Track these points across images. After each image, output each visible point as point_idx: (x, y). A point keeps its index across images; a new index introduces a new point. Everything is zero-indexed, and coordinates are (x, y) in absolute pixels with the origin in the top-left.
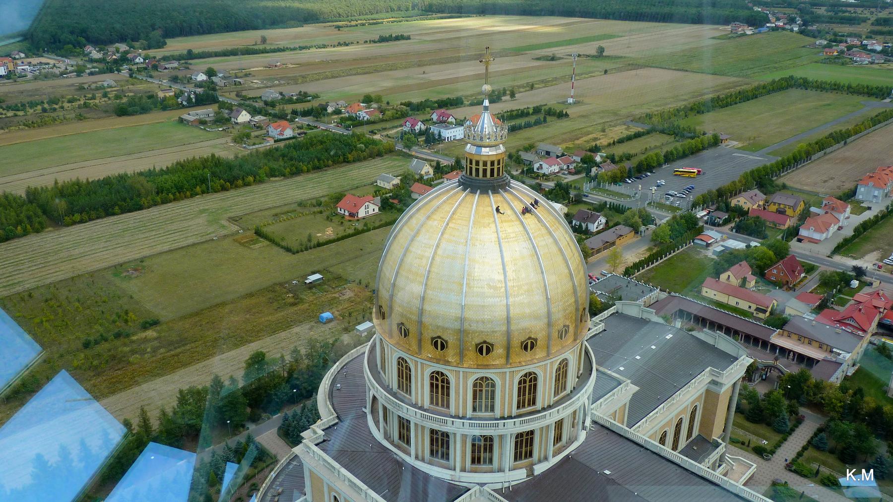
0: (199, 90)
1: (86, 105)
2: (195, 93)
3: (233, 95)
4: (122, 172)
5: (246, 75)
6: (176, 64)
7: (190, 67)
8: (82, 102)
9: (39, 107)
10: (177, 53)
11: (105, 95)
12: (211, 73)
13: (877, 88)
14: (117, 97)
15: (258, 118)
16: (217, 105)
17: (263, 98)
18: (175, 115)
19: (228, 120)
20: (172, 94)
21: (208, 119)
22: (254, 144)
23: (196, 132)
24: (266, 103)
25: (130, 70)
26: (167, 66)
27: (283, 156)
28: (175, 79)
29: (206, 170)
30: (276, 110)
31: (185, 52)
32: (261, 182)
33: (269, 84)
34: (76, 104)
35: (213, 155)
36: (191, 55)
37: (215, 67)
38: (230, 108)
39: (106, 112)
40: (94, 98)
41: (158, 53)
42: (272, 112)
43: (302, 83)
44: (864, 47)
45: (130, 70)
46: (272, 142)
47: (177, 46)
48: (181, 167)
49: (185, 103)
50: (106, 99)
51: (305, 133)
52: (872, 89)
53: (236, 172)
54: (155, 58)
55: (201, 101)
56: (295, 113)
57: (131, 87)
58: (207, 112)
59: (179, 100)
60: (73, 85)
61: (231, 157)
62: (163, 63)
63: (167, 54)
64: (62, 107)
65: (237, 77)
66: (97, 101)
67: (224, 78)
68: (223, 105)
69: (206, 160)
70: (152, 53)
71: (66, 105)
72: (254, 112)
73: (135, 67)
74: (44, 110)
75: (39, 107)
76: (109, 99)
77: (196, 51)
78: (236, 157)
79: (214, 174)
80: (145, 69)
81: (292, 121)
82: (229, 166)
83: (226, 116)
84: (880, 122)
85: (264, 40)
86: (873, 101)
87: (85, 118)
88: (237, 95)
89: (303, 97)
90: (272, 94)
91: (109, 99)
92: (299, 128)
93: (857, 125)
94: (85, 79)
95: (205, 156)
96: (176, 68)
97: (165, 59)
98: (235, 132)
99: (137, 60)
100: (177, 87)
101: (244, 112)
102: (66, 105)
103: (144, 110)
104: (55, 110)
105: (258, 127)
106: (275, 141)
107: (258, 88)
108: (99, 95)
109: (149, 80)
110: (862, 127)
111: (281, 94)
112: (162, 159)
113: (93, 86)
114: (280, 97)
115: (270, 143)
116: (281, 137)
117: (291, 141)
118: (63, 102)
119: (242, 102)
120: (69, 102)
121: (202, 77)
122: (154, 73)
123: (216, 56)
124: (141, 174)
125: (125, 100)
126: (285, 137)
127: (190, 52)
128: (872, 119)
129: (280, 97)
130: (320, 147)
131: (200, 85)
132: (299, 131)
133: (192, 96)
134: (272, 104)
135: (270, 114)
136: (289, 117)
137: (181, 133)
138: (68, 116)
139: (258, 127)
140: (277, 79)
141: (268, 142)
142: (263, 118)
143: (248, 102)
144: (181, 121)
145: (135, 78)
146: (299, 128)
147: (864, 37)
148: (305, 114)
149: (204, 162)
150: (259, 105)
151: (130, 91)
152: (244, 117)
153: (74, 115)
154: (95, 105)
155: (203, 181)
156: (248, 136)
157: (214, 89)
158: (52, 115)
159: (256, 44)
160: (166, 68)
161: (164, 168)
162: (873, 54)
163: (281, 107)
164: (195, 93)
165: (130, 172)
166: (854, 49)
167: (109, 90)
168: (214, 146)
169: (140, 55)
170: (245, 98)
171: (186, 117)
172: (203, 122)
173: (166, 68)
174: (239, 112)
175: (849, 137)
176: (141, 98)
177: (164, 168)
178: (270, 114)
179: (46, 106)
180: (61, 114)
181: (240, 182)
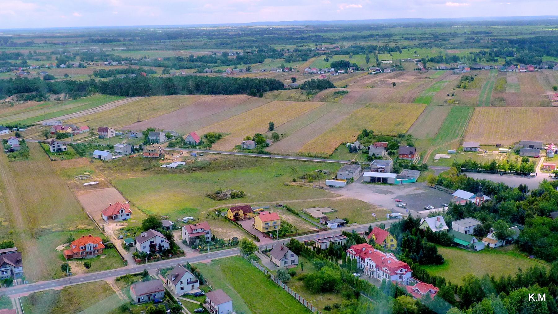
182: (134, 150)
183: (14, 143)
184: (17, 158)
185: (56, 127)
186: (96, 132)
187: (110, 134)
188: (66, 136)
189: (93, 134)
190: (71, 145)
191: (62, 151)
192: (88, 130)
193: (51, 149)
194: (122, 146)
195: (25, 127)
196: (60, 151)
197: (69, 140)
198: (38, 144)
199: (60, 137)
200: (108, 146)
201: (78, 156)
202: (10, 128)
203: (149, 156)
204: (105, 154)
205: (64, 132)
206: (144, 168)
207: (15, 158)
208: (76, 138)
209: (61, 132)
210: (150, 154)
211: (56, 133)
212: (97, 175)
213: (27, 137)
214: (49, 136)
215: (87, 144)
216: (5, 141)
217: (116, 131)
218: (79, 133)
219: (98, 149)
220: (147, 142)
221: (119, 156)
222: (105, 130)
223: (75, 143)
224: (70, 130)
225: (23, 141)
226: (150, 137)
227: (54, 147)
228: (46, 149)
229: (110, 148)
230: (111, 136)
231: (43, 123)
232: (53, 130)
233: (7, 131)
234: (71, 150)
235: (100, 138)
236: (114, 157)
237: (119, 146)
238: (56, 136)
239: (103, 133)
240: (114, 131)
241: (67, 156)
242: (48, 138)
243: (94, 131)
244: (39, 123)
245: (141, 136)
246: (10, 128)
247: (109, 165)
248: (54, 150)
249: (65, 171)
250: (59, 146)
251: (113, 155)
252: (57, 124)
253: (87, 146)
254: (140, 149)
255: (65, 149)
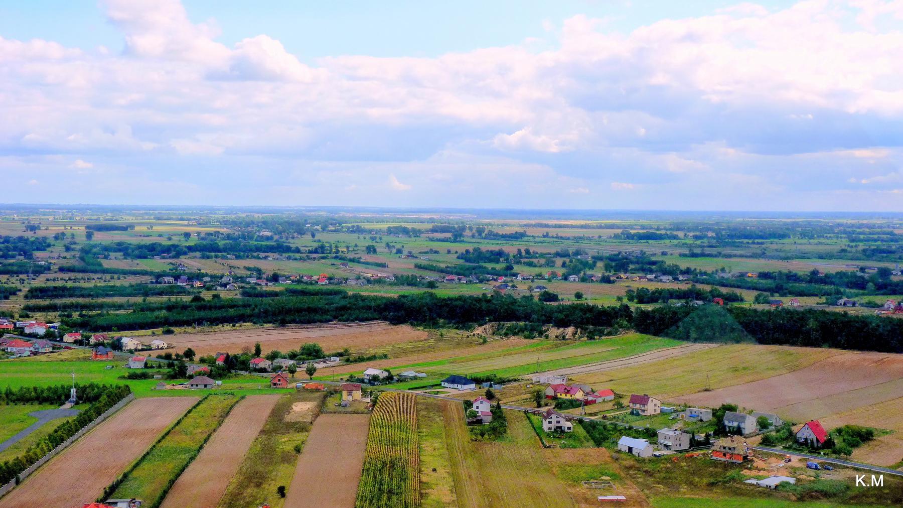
13: (49, 389)
44: (21, 331)
52: (42, 391)
84: (62, 440)
86: (48, 408)
93: (29, 450)
110: (38, 451)
128: (50, 436)
147: (17, 316)
162: (34, 340)
166: (6, 336)
175: (21, 470)
182: (695, 444)
183: (483, 408)
184: (486, 436)
185: (556, 388)
186: (625, 402)
187: (651, 408)
188: (574, 404)
189: (620, 406)
190: (581, 422)
191: (563, 432)
192: (612, 397)
193: (545, 425)
194: (672, 433)
195: (502, 382)
196: (559, 432)
197: (576, 412)
198: (523, 415)
199: (561, 405)
200: (647, 430)
201: (592, 443)
202: (477, 381)
203: (723, 459)
204: (641, 446)
205: (569, 397)
206: (712, 480)
207: (482, 435)
208: (590, 409)
209: (563, 396)
210: (725, 455)
211: (555, 398)
212: (623, 484)
213: (505, 401)
214: (542, 403)
215: (608, 422)
216: (468, 404)
217: (663, 404)
218: (594, 402)
219: (629, 435)
220: (721, 431)
221: (665, 452)
222: (643, 400)
223: (587, 419)
224: (579, 395)
225: (499, 406)
226: (727, 423)
227: (550, 422)
228: (536, 424)
229: (651, 435)
230: (653, 413)
231: (534, 378)
232: (550, 392)
233: (473, 386)
234: (581, 431)
235: (632, 413)
236: (657, 453)
237: (667, 434)
238: (554, 403)
239: (638, 406)
240: (659, 403)
241: (572, 442)
242: (539, 406)
243: (622, 401)
244: (527, 377)
245: (708, 417)
246: (477, 381)
247: (648, 467)
248: (550, 428)
249: (568, 469)
250: (558, 422)
251: (655, 450)
252: (558, 382)
253: (609, 427)
254: (706, 443)
255: (569, 428)
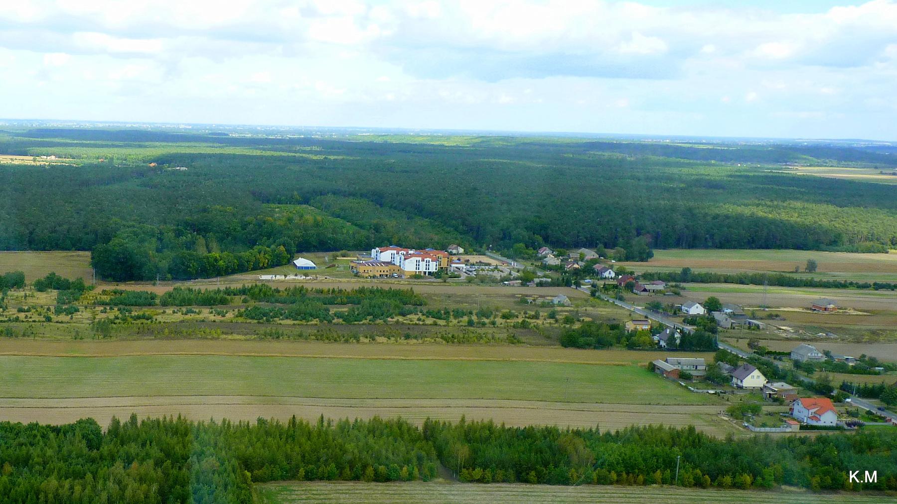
0: (689, 328)
1: (524, 325)
2: (682, 332)
3: (744, 343)
4: (551, 424)
5: (771, 317)
6: (660, 286)
7: (682, 293)
8: (520, 320)
9: (466, 319)
10: (667, 271)
11: (552, 316)
12: (712, 306)
14: (568, 320)
15: (777, 386)
16: (713, 354)
17: (794, 356)
18: (644, 358)
19: (727, 380)
20: (647, 327)
21: (694, 373)
22: (764, 425)
23: (672, 389)
24: (797, 364)
25: (594, 286)
26: (647, 287)
27: (813, 455)
28: (655, 308)
29: (676, 449)
30: (815, 378)
31: (679, 271)
32: (764, 487)
33: (809, 335)
34: (512, 321)
35: (691, 429)
36: (686, 276)
37: (722, 298)
38: (734, 361)
39: (548, 337)
40: (536, 317)
41: (637, 268)
42: (806, 380)
43: (870, 342)
45: (594, 286)
46: (795, 427)
47: (667, 260)
48: (639, 436)
49: (663, 343)
50: (552, 321)
51: (860, 425)
53: (725, 462)
54: (632, 273)
55: (688, 344)
56: (846, 389)
57: (589, 309)
58: (695, 362)
59: (656, 338)
60: (513, 296)
61: (721, 437)
62: (641, 282)
63: (651, 270)
64: (493, 323)
65: (754, 318)
66: (540, 322)
67: (733, 315)
68: (723, 356)
69: (679, 434)
70: (629, 266)
71: (499, 320)
72: (772, 375)
73: (601, 283)
74: (471, 323)
75: (466, 319)
76: (557, 321)
77: (695, 271)
78: (730, 440)
79: (687, 458)
80: (615, 287)
81: (838, 400)
82: (716, 451)
83: (725, 373)
85: (812, 267)
87: (519, 342)
88: (750, 345)
89: (867, 366)
90: (812, 352)
91: (557, 321)
92: (849, 414)
94: (532, 290)
95: (679, 428)
96: (660, 292)
97: (648, 277)
98: (735, 400)
99: (606, 274)
100: (655, 319)
101: (756, 373)
102: (499, 320)
103: (601, 344)
104: (484, 324)
105: (775, 400)
106: (802, 428)
107: (787, 339)
108: (543, 313)
109: (618, 303)
111: (827, 354)
112: (613, 419)
113: (540, 301)
114: (824, 359)
115: (793, 429)
116: (815, 423)
117: (831, 433)
118: (496, 316)
119: (757, 356)
120: (504, 317)
121: (697, 310)
122: (626, 295)
123: (726, 282)
124: (577, 433)
125: (577, 326)
126: (821, 424)
127: (686, 271)
129: (824, 359)
130: (885, 454)
131: (692, 320)
132: (850, 420)
133: (677, 335)
134: (809, 368)
135: (800, 384)
136: (835, 393)
137: (649, 386)
138: (497, 336)
139: (775, 400)
140: (822, 330)
141: (789, 426)
142: (787, 386)
143: (765, 358)
144: (653, 368)
145: (598, 298)
146: (849, 414)
148: (868, 393)
149: (675, 437)
150: (784, 365)
151: (588, 315)
152: (755, 380)
153: (505, 335)
154: (537, 327)
155: (669, 464)
156: (755, 411)
157: (714, 331)
158: (479, 331)
159: (796, 272)
160: (645, 290)
161: (613, 432)
163: (824, 374)
164: (682, 332)
165: (562, 427)
167: (559, 309)
168: (696, 416)
169: (611, 267)
170: (762, 352)
171: (661, 363)
172: (684, 376)
173: (645, 290)
174: (747, 371)
176: (599, 327)
177: (613, 432)
178: (800, 384)
179: (474, 318)
180: (490, 331)
181: (728, 479)
